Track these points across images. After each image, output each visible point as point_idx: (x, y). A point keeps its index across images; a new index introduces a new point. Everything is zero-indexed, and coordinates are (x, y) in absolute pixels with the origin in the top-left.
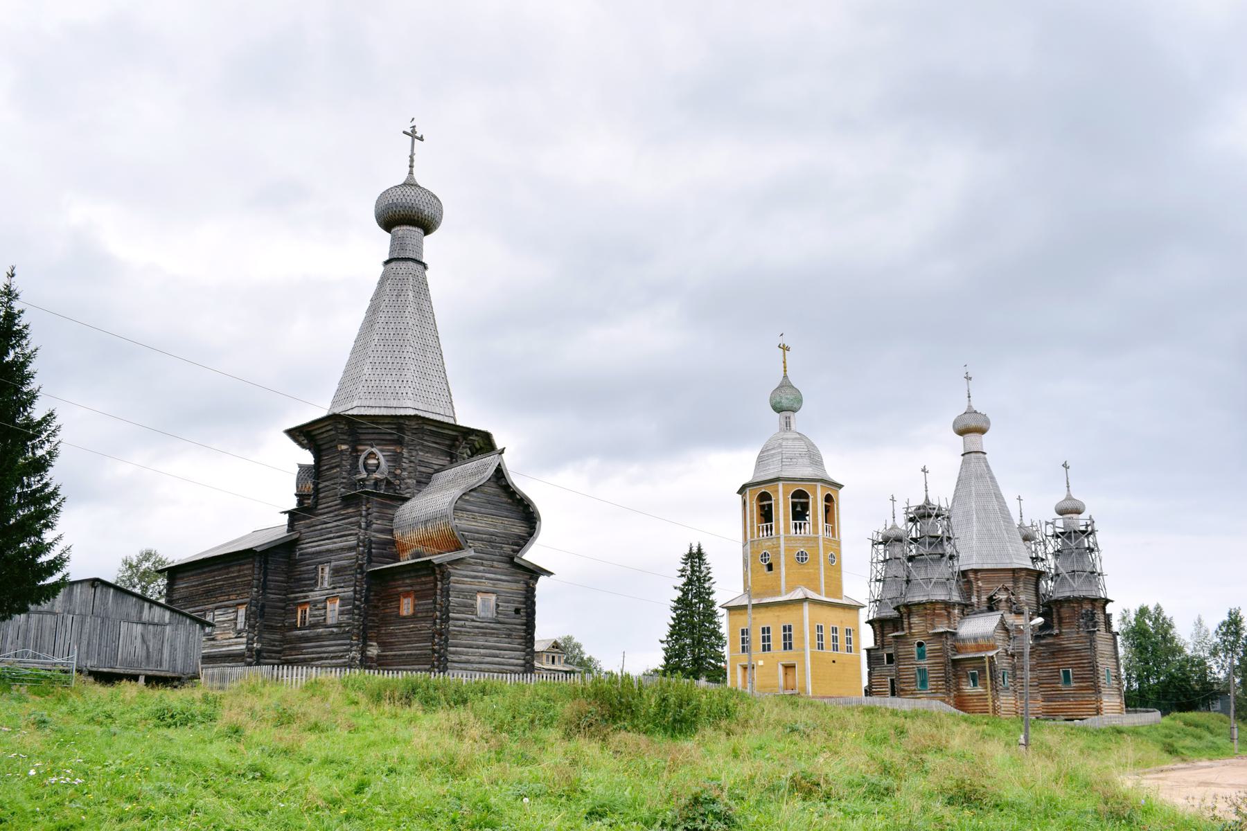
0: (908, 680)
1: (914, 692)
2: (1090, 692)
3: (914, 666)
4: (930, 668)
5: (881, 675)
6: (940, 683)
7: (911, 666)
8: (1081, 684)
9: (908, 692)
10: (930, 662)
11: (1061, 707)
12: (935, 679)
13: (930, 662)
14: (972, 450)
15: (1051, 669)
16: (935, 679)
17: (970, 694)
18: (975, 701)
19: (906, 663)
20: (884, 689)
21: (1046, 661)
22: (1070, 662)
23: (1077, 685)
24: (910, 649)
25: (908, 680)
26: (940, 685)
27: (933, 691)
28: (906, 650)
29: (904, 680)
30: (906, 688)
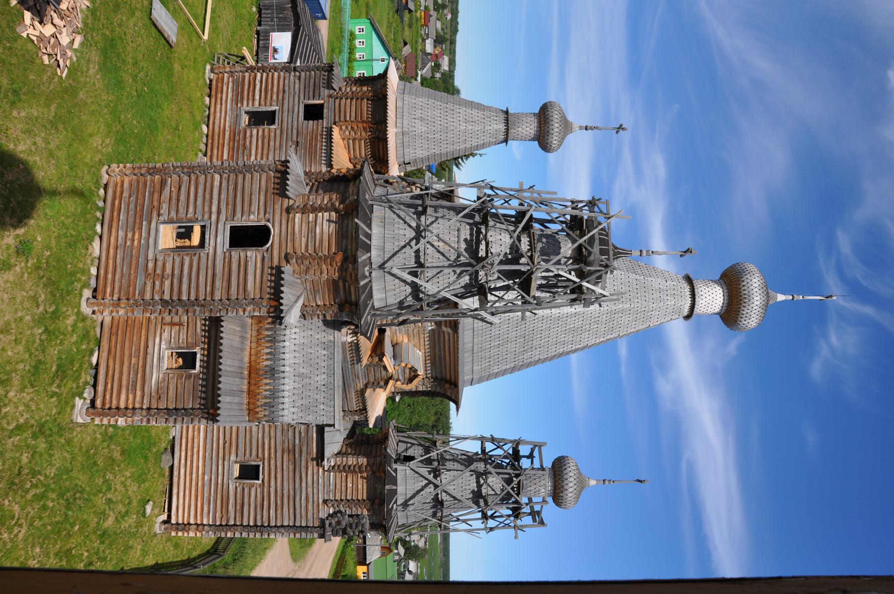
1: (155, 214)
2: (218, 515)
3: (214, 217)
4: (204, 260)
5: (284, 92)
6: (167, 283)
7: (214, 208)
8: (232, 501)
9: (156, 196)
10: (219, 262)
11: (195, 456)
12: (177, 272)
13: (219, 262)
14: (697, 299)
15: (264, 444)
16: (177, 272)
17: (150, 350)
18: (134, 360)
19: (223, 196)
20: (257, 97)
21: (279, 434)
22: (273, 483)
23: (232, 492)
24: (254, 208)
25: (183, 198)
26: (162, 283)
28: (255, 198)
29: (183, 189)
30: (166, 192)
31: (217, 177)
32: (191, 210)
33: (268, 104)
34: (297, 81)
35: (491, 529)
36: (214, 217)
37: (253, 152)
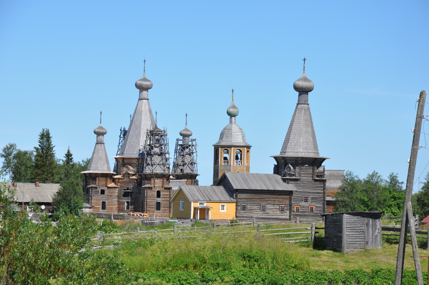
0: (151, 206)
3: (155, 201)
7: (154, 200)
12: (164, 207)
16: (164, 207)
20: (98, 206)
24: (154, 193)
25: (151, 206)
27: (163, 212)
28: (152, 193)
29: (150, 206)
31: (148, 200)
32: (153, 205)
33: (100, 203)
34: (95, 196)
35: (196, 151)
36: (155, 201)
37: (112, 207)
